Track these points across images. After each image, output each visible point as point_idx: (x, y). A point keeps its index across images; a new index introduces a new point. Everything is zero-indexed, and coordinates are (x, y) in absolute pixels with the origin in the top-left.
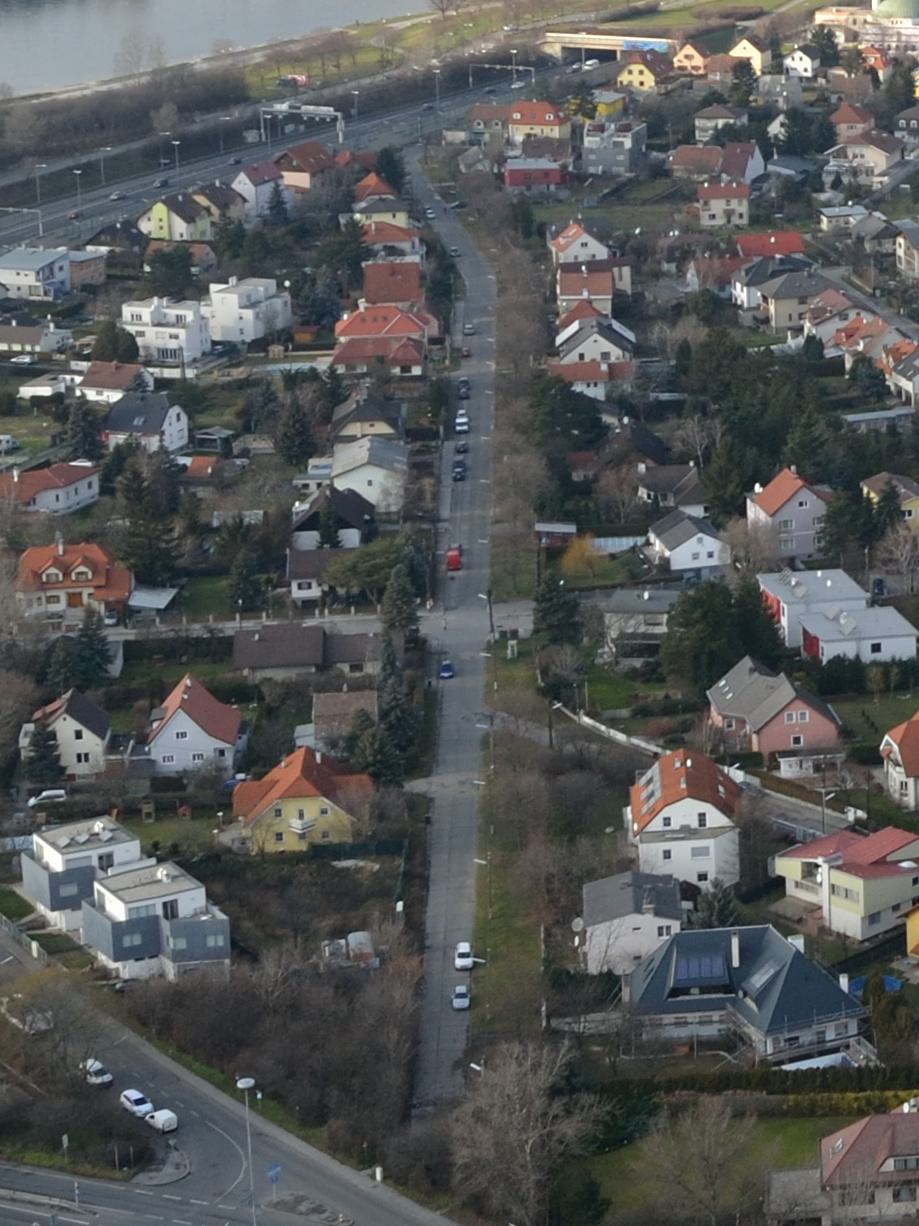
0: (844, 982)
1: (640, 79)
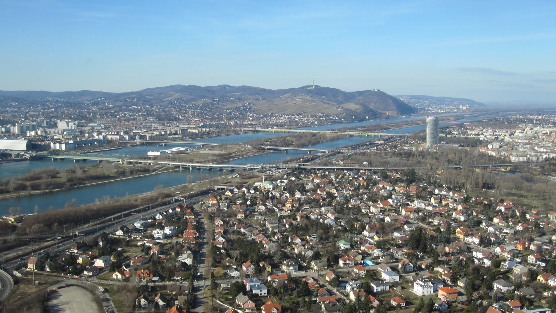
1: (228, 193)
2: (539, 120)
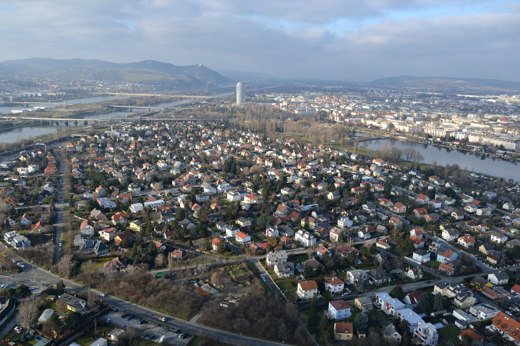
0: (107, 246)
1: (83, 140)
2: (315, 88)
